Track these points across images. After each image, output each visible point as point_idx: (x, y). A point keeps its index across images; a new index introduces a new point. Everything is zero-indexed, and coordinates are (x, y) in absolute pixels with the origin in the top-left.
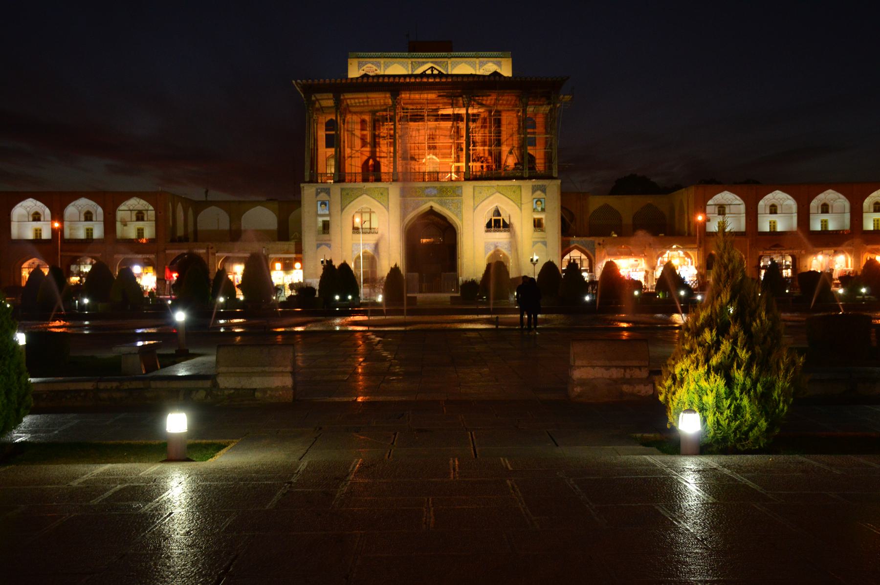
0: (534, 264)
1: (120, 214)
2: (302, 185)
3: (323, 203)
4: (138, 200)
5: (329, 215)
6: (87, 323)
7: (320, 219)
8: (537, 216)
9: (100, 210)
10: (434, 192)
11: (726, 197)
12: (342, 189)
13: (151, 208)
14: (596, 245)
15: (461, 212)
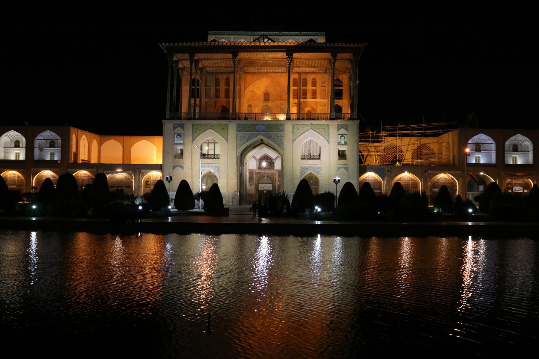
0: (337, 184)
1: (37, 143)
2: (163, 121)
3: (179, 135)
4: (51, 132)
5: (183, 144)
6: (34, 219)
7: (179, 148)
8: (342, 148)
9: (24, 140)
10: (263, 128)
11: (482, 138)
12: (193, 125)
13: (59, 138)
14: (386, 172)
15: (283, 143)
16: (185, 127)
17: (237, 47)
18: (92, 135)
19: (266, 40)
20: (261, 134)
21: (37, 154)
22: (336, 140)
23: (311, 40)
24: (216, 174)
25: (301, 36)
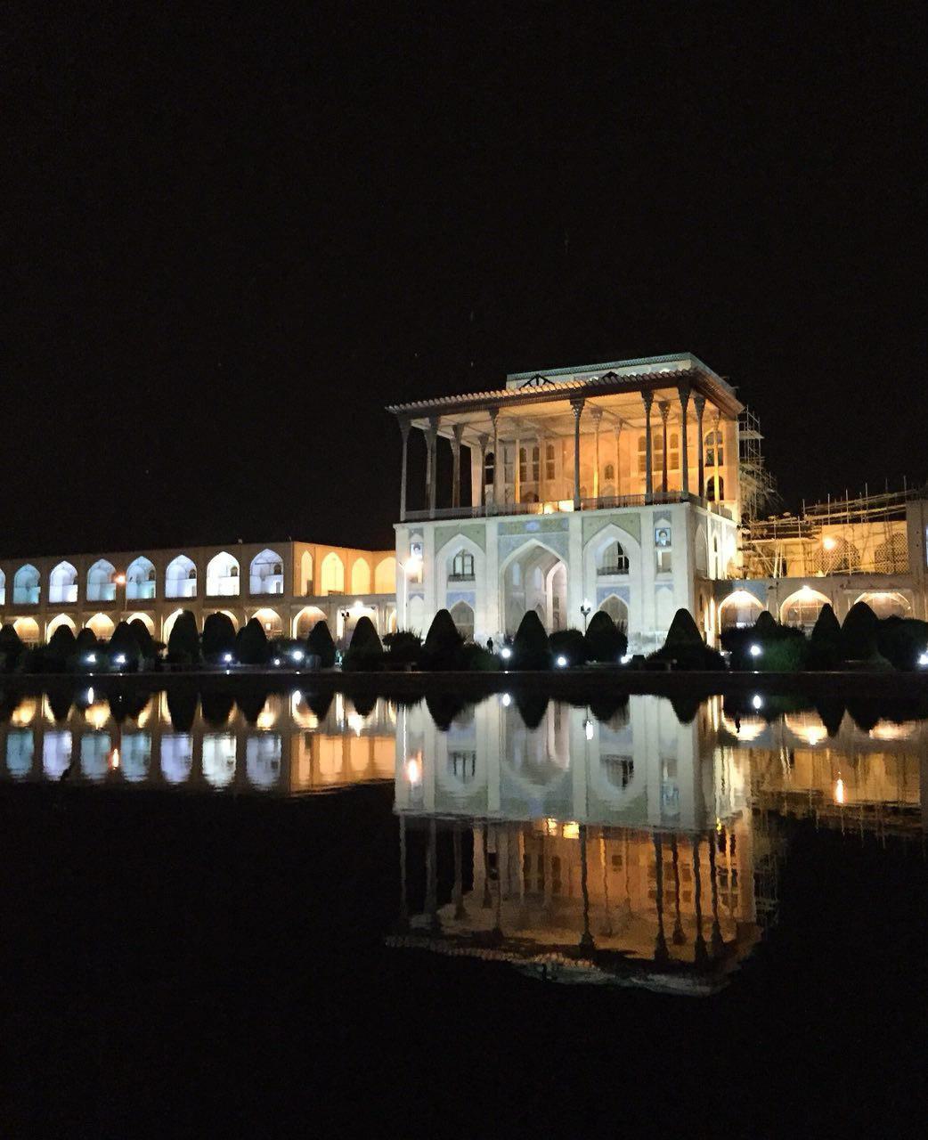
1: (255, 569)
2: (395, 526)
3: (417, 546)
10: (537, 526)
12: (436, 529)
15: (567, 549)
16: (425, 534)
17: (496, 400)
18: (351, 552)
19: (541, 381)
20: (535, 537)
21: (256, 586)
22: (651, 539)
23: (611, 374)
24: (469, 605)
25: (649, 364)
